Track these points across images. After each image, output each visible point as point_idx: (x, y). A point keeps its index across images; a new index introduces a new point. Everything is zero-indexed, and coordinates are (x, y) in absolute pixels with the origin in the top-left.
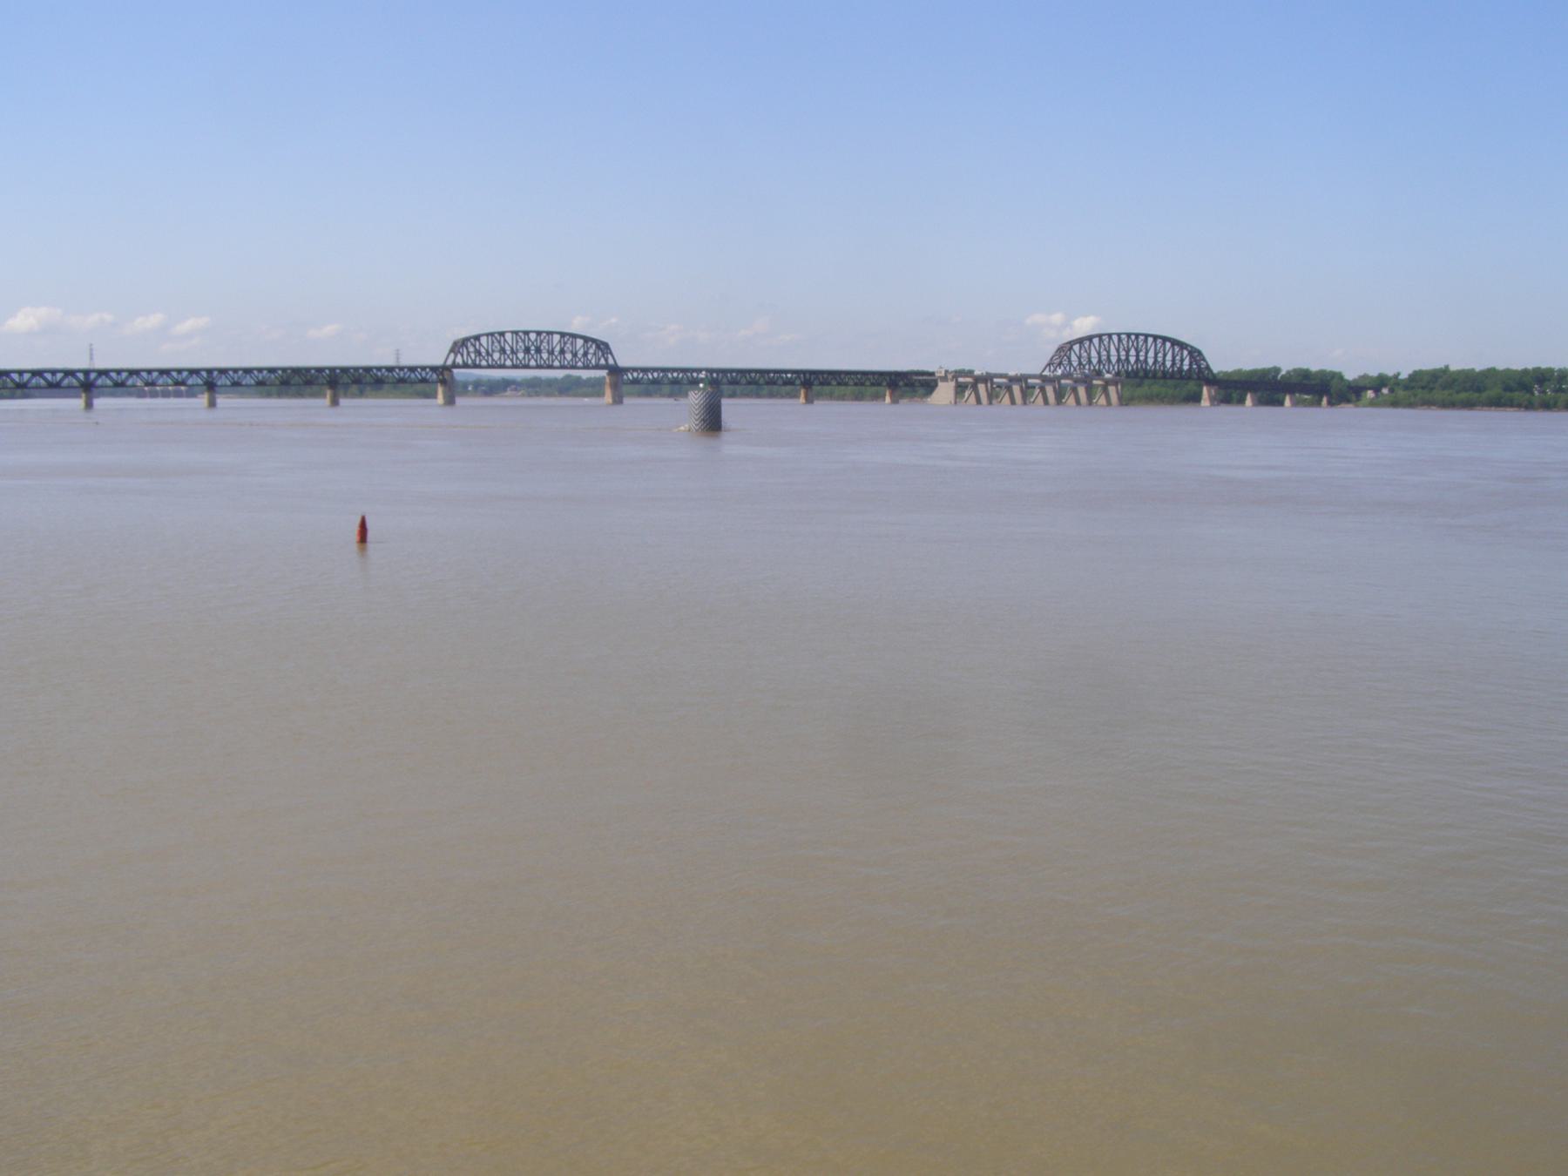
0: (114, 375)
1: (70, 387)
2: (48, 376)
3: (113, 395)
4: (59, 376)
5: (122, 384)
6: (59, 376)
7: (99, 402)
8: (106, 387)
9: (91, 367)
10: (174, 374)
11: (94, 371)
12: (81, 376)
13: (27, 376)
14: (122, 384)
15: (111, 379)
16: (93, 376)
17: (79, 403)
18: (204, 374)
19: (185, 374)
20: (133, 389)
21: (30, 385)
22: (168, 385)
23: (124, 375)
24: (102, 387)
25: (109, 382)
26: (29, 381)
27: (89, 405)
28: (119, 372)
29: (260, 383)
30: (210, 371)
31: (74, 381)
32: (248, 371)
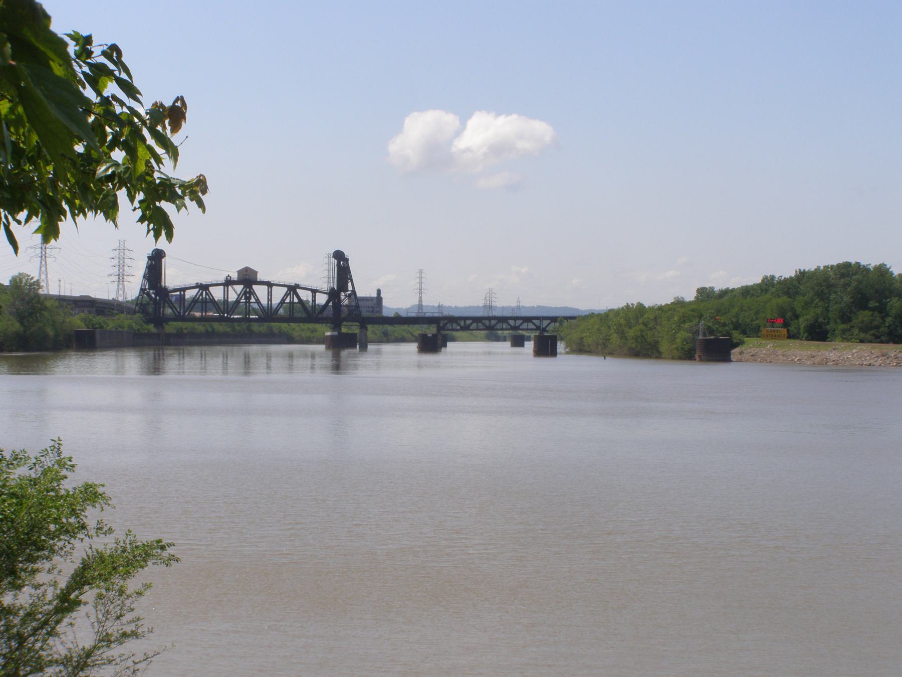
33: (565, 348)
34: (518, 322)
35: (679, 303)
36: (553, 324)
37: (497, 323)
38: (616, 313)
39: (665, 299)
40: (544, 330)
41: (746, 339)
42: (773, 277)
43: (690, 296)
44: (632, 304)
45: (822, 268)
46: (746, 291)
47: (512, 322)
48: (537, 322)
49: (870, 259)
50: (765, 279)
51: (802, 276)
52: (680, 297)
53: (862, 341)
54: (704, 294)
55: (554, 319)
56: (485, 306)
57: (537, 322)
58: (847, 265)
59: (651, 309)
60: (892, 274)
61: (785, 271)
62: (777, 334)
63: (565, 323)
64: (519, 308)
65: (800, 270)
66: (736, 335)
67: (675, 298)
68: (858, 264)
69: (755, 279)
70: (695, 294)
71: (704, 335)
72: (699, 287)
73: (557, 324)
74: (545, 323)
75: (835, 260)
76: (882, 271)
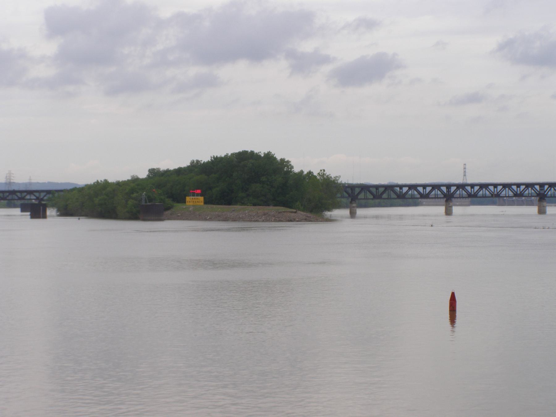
0: (492, 188)
1: (484, 196)
2: (469, 188)
3: (494, 203)
4: (476, 188)
5: (521, 195)
6: (428, 189)
7: (456, 210)
8: (486, 197)
9: (465, 182)
10: (514, 187)
11: (454, 185)
12: (444, 189)
13: (405, 189)
14: (475, 196)
15: (513, 191)
16: (453, 189)
17: (534, 209)
18: (537, 187)
19: (500, 188)
20: (410, 200)
21: (407, 196)
22: (532, 196)
23: (476, 188)
24: (504, 197)
25: (511, 194)
26: (407, 192)
27: (448, 212)
28: (518, 185)
29: (470, 196)
30: (542, 185)
31: (416, 193)
32: (506, 186)
33: (57, 212)
34: (24, 194)
35: (135, 180)
36: (48, 196)
37: (9, 195)
38: (89, 187)
39: (125, 177)
40: (42, 200)
41: (175, 204)
42: (198, 161)
43: (143, 174)
44: (101, 181)
45: (230, 154)
46: (179, 171)
47: (19, 194)
48: (37, 194)
49: (261, 149)
50: (192, 162)
51: (216, 161)
52: (135, 176)
53: (255, 205)
54: (154, 173)
55: (48, 192)
56: (6, 183)
57: (37, 194)
58: (244, 153)
59: (112, 184)
60: (275, 159)
61: (205, 158)
62: (197, 200)
63: (56, 195)
64: (30, 184)
65: (214, 156)
66: (169, 201)
67: (132, 176)
68: (252, 152)
69: (185, 163)
70: (147, 173)
71: (146, 202)
72: (150, 168)
73: (51, 196)
74: (42, 194)
75: (237, 150)
76: (269, 157)
